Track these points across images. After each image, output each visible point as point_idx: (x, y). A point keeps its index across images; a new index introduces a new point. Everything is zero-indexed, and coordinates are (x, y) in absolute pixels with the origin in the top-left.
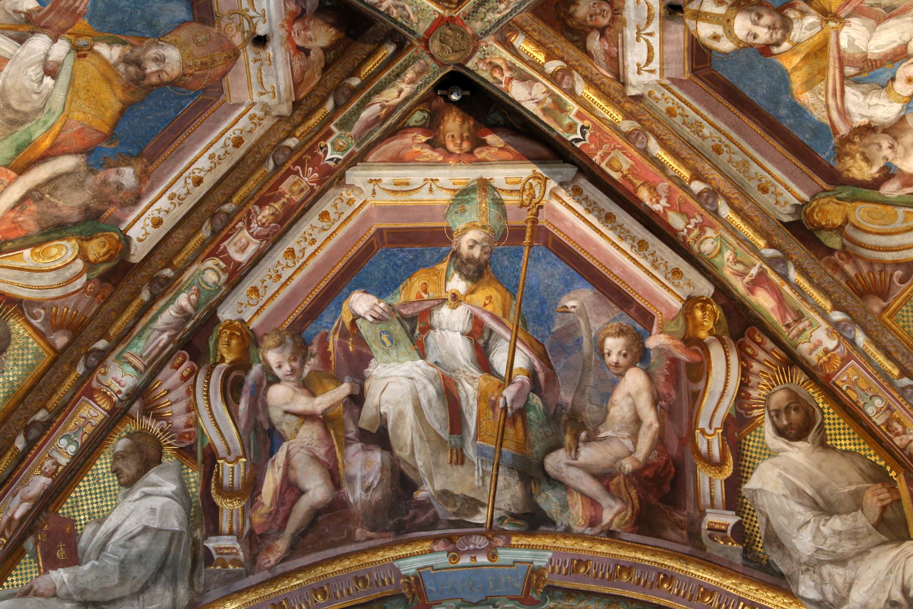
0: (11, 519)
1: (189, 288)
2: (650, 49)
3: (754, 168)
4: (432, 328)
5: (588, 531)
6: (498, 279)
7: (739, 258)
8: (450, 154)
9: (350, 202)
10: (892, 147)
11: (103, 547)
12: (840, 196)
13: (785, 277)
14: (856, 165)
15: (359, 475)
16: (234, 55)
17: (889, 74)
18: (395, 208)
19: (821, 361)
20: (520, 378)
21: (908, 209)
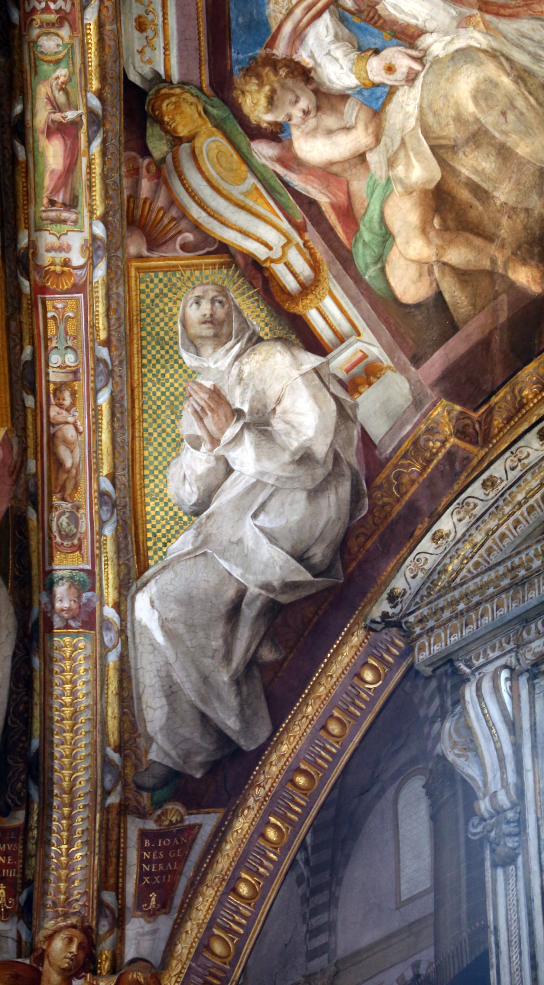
7: (69, 88)
10: (306, 113)
12: (210, 108)
14: (256, 96)
17: (374, 42)
19: (52, 268)
21: (259, 186)
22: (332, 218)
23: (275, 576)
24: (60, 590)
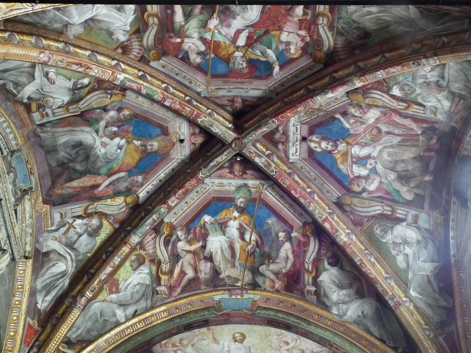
0: (101, 280)
1: (155, 213)
2: (296, 149)
3: (326, 186)
4: (228, 227)
5: (271, 290)
6: (248, 213)
8: (236, 176)
9: (205, 188)
10: (365, 183)
11: (126, 288)
13: (333, 219)
15: (203, 270)
16: (174, 144)
18: (219, 191)
20: (253, 243)
22: (386, 196)
23: (431, 268)
24: (390, 302)
